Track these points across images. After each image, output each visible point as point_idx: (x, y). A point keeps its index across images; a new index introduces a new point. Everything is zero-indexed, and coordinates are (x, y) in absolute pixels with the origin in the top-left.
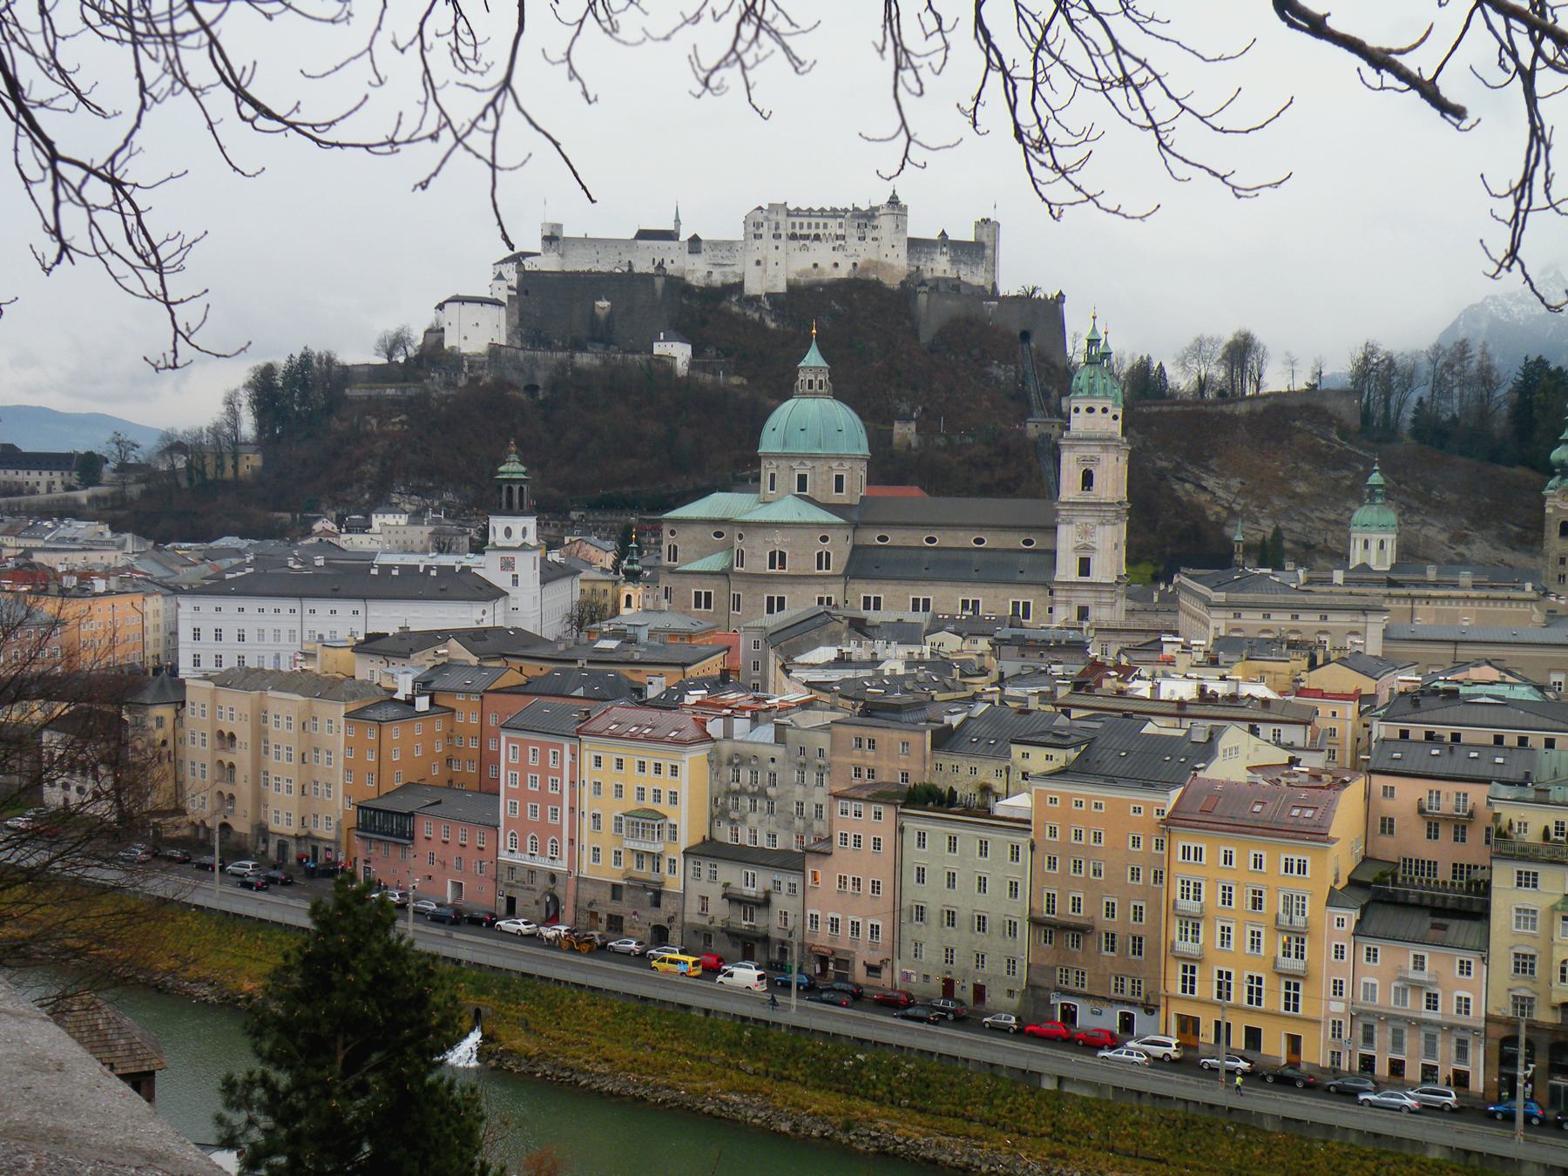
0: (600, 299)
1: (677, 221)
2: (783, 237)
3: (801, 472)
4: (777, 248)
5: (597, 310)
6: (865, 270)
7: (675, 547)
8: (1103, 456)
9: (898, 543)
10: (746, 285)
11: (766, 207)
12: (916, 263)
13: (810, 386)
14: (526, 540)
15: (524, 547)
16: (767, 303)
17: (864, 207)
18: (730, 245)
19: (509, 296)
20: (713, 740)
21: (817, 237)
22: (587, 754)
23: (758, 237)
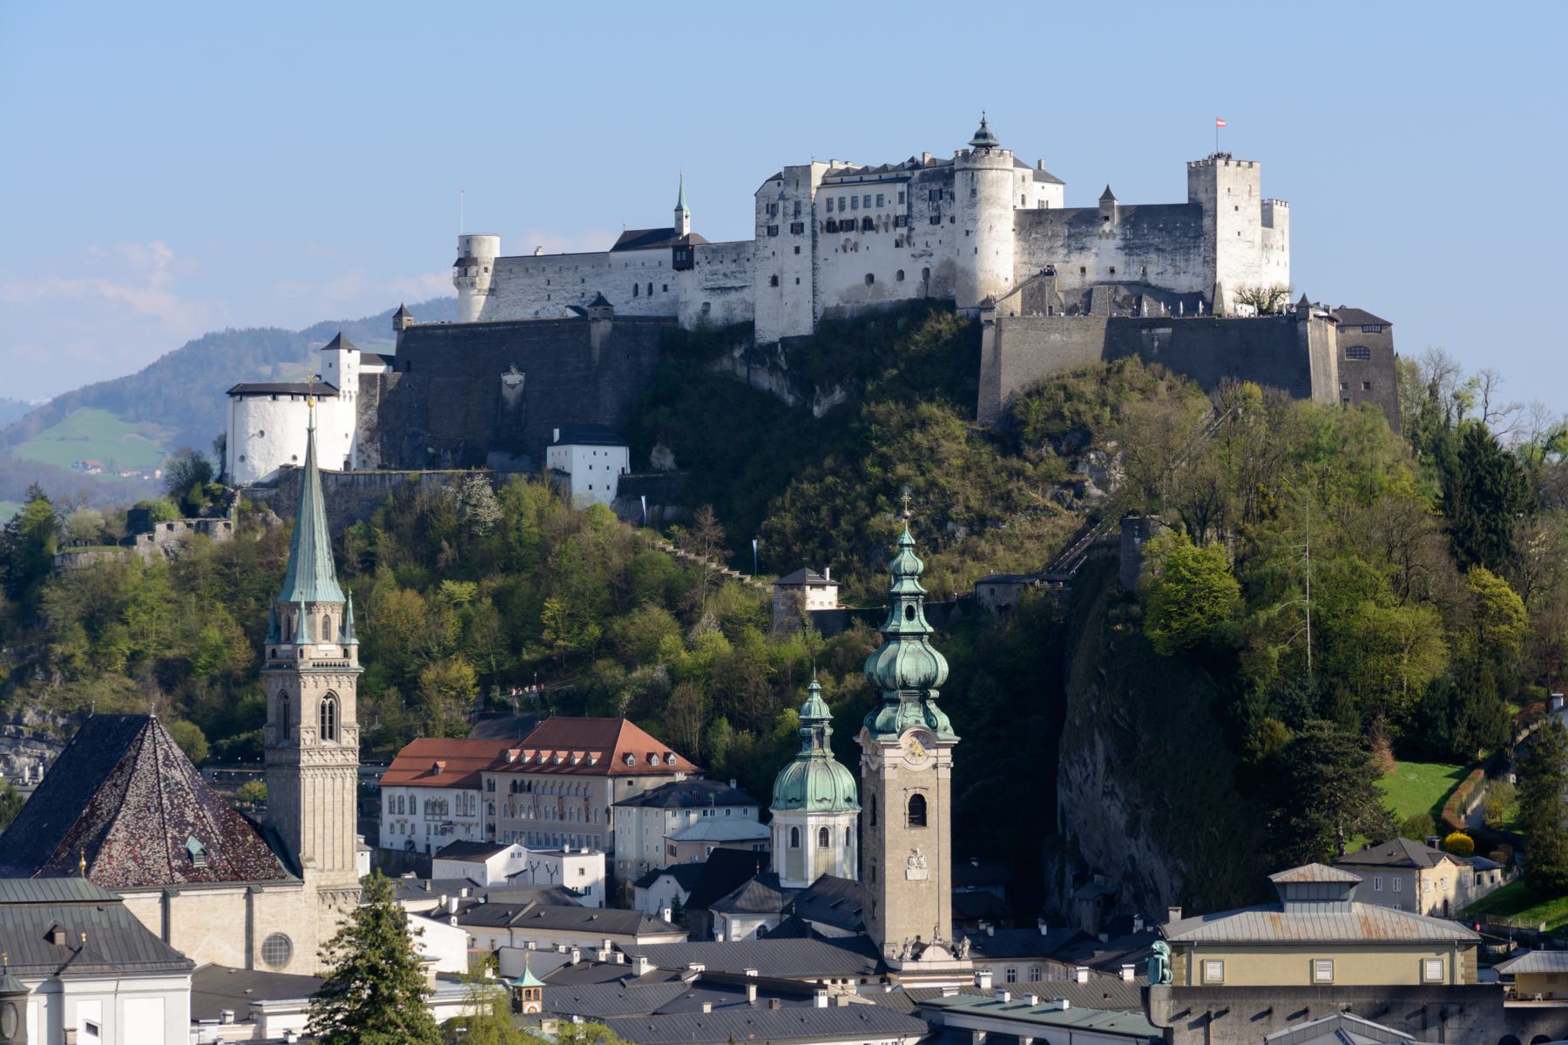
0: (508, 371)
1: (679, 209)
2: (807, 230)
4: (797, 250)
5: (506, 392)
10: (759, 325)
12: (1044, 259)
16: (782, 361)
18: (736, 251)
19: (361, 376)
21: (868, 225)
23: (773, 231)
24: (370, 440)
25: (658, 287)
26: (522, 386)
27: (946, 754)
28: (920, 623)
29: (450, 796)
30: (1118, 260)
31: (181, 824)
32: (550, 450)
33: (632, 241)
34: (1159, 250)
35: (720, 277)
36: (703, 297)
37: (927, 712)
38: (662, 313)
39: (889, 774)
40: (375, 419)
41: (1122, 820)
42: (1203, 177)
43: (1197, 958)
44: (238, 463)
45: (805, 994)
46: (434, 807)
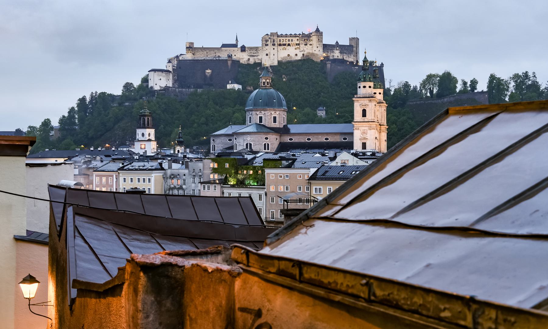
0: (207, 69)
1: (237, 40)
3: (261, 116)
4: (274, 49)
6: (307, 56)
7: (214, 146)
8: (370, 104)
9: (297, 141)
11: (269, 34)
13: (264, 84)
14: (150, 138)
15: (149, 140)
16: (271, 70)
17: (306, 33)
18: (256, 49)
20: (164, 170)
21: (289, 45)
22: (121, 177)
23: (267, 45)
24: (175, 82)
26: (211, 73)
30: (339, 55)
32: (228, 85)
34: (346, 53)
35: (252, 53)
36: (248, 57)
40: (176, 78)
42: (353, 41)
44: (155, 85)
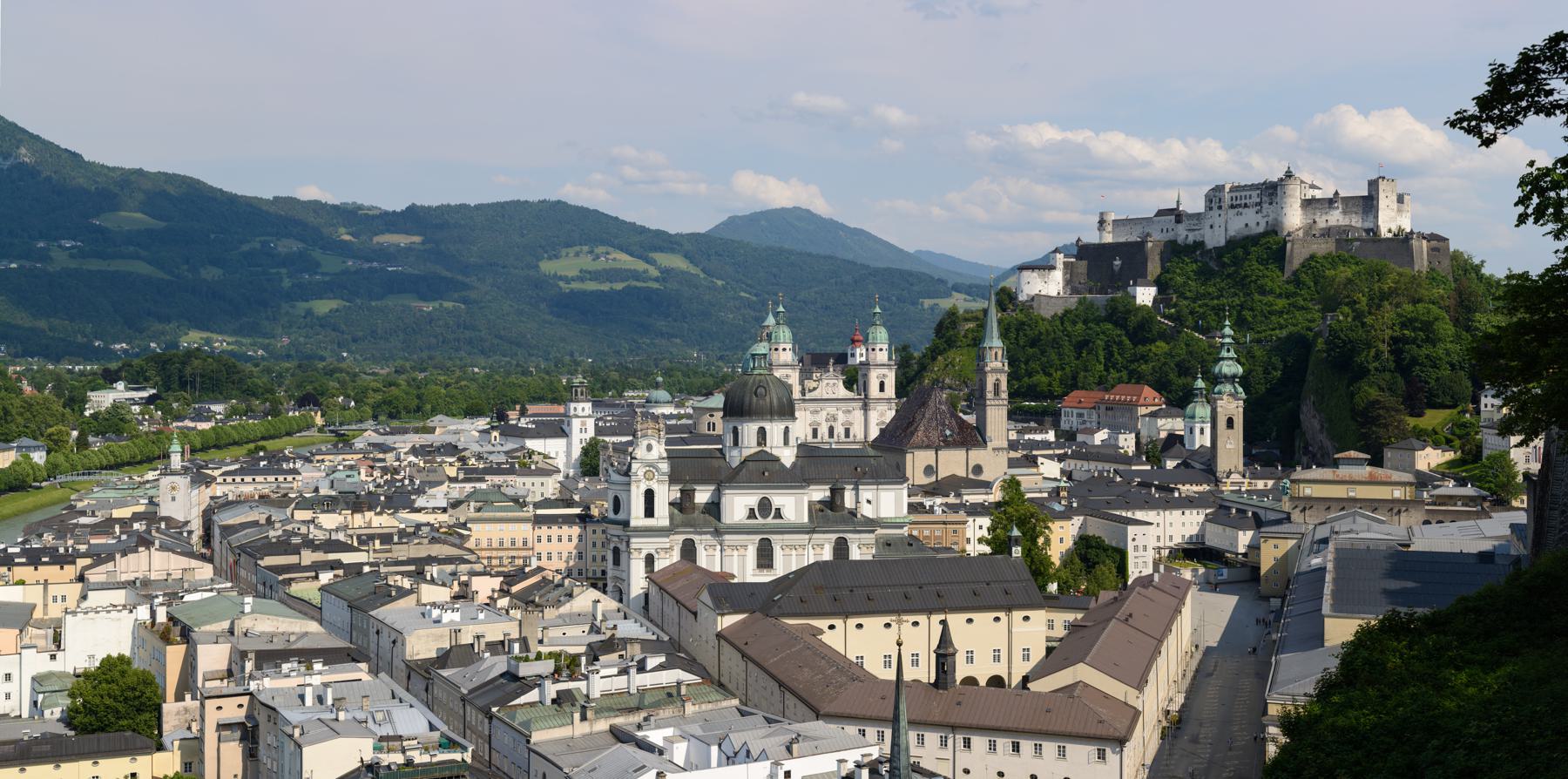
10: (1207, 242)
18: (1198, 216)
21: (1246, 206)
23: (1211, 209)
25: (1170, 230)
27: (1241, 403)
28: (1232, 354)
29: (1085, 412)
30: (1341, 218)
31: (944, 425)
33: (1161, 213)
36: (1186, 233)
37: (1235, 387)
38: (1173, 239)
39: (1219, 409)
41: (1318, 427)
43: (1302, 486)
45: (1172, 490)
46: (1080, 415)
